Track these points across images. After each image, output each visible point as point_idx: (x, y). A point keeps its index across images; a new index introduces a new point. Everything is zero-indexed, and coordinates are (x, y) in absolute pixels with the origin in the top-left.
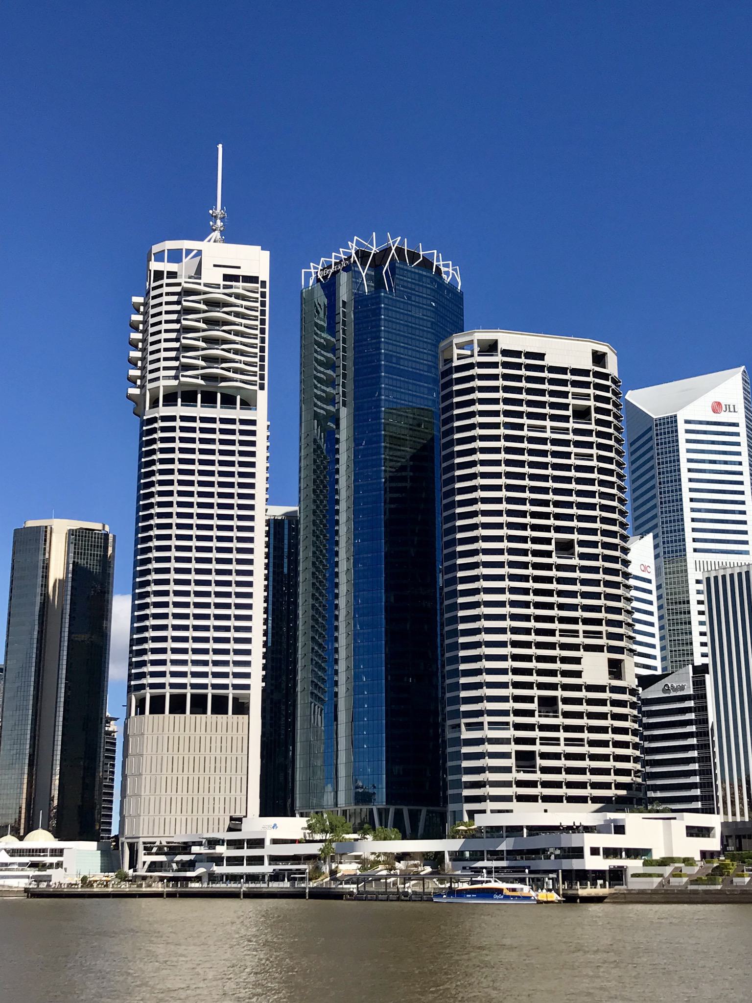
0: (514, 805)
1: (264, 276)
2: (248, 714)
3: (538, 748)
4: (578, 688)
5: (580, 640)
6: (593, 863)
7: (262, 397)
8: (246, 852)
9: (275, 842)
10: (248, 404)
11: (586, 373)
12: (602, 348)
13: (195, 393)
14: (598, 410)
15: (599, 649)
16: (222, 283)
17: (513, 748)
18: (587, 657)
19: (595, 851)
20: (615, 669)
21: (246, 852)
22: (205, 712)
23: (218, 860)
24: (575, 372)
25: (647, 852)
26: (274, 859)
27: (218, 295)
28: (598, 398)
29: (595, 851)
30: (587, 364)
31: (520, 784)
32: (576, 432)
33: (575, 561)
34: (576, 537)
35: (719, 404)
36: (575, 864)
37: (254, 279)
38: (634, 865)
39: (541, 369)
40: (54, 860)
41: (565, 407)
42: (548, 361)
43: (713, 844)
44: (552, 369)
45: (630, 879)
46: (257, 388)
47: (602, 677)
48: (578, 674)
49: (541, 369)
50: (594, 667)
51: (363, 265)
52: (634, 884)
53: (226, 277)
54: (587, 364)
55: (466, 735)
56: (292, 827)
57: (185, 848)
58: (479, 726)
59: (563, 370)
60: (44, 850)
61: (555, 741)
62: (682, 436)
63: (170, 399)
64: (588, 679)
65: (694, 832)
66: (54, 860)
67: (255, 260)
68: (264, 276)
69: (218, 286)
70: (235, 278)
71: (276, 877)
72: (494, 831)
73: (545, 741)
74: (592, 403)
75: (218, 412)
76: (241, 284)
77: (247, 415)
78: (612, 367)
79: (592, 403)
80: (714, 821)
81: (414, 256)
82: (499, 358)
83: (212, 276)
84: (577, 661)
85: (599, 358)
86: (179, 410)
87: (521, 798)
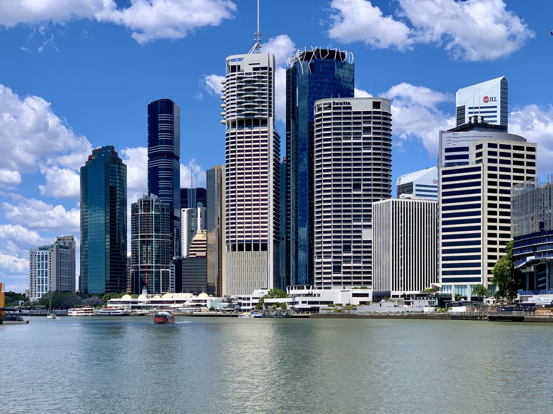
0: (332, 286)
2: (267, 250)
4: (360, 242)
8: (246, 302)
9: (253, 298)
11: (369, 113)
13: (243, 120)
16: (253, 72)
18: (364, 231)
19: (304, 302)
21: (246, 302)
22: (243, 250)
24: (365, 113)
25: (332, 302)
26: (253, 304)
29: (304, 302)
30: (370, 108)
31: (335, 278)
35: (486, 97)
39: (350, 113)
41: (360, 128)
44: (355, 113)
45: (320, 311)
46: (267, 117)
48: (360, 237)
53: (255, 69)
58: (320, 257)
59: (359, 113)
60: (202, 300)
64: (364, 239)
65: (355, 295)
66: (203, 304)
69: (250, 74)
70: (257, 69)
76: (260, 71)
79: (372, 125)
84: (360, 231)
87: (334, 283)
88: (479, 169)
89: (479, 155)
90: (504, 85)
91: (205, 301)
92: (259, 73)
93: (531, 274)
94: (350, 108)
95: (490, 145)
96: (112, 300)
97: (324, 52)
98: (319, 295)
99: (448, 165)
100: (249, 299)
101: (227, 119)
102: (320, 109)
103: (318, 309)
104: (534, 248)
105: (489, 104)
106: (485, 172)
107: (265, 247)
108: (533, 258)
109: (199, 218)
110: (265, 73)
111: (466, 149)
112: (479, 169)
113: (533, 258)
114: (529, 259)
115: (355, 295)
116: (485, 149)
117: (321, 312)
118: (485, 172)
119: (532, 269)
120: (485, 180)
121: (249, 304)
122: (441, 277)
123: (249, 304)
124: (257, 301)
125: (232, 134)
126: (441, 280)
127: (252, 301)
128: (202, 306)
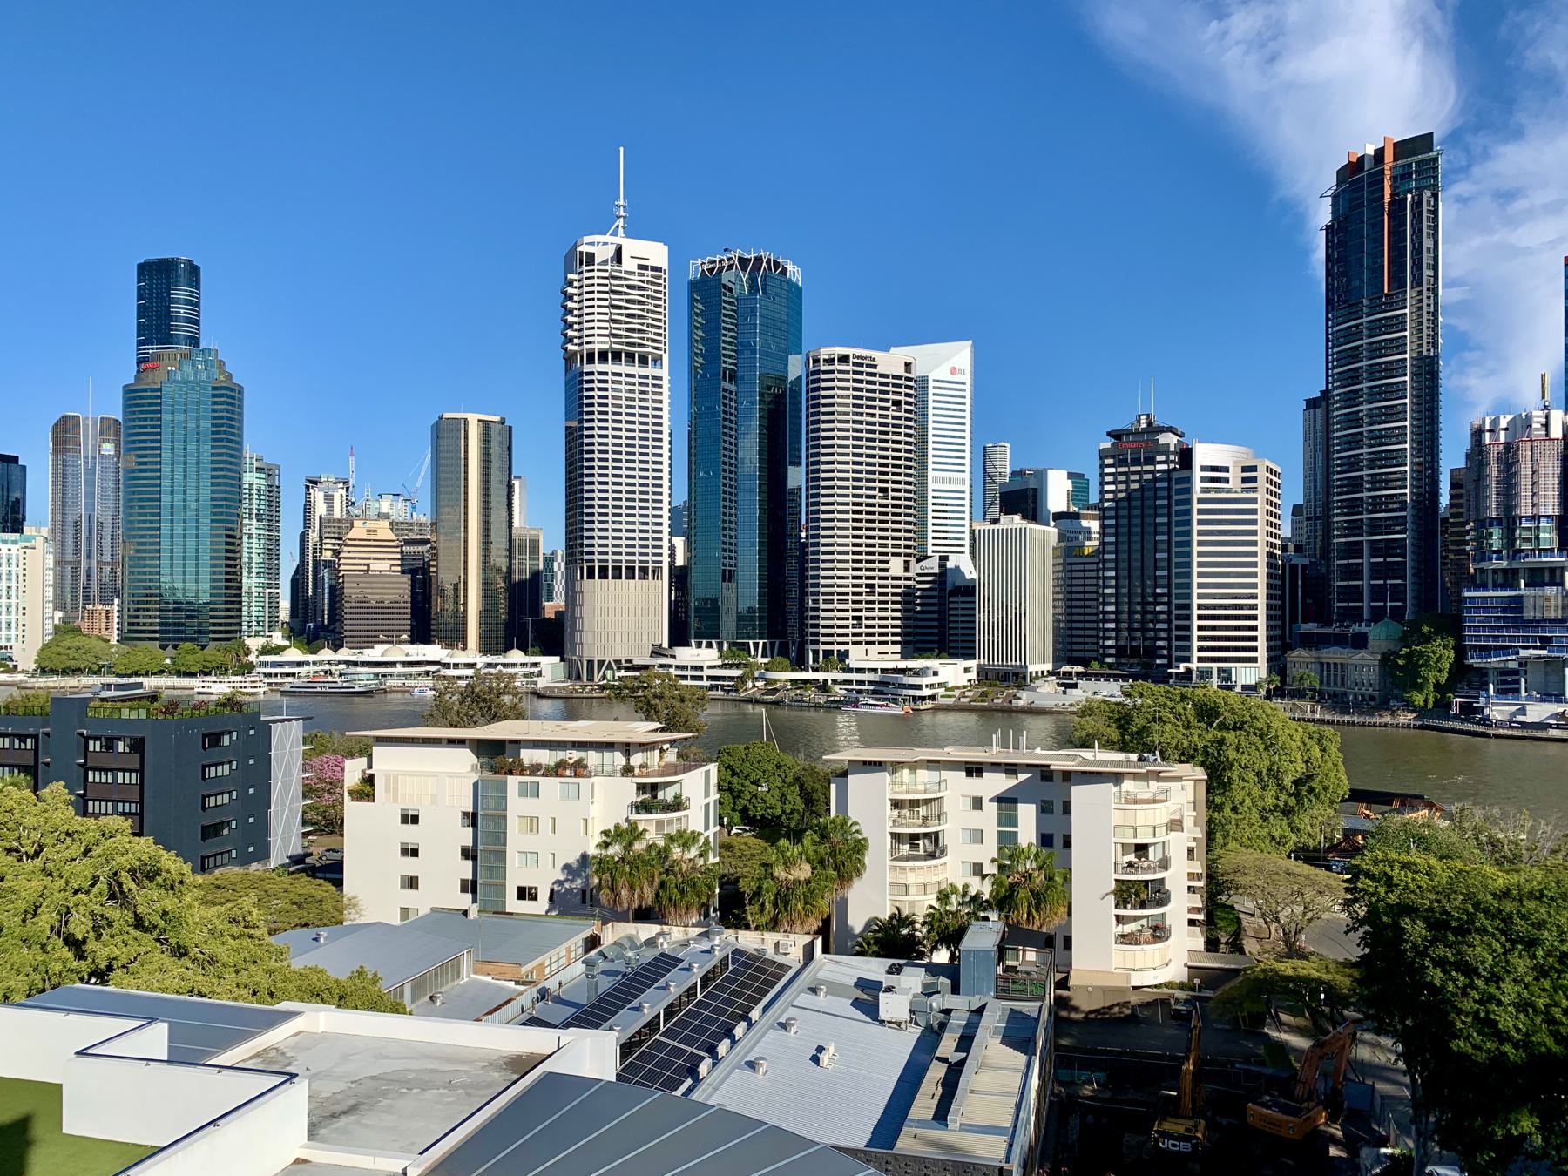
1: (665, 266)
3: (864, 614)
7: (666, 358)
9: (710, 667)
10: (657, 360)
11: (900, 378)
12: (909, 360)
14: (907, 403)
15: (899, 555)
17: (851, 614)
24: (894, 377)
26: (709, 678)
27: (635, 280)
28: (907, 395)
32: (894, 418)
33: (890, 501)
34: (890, 486)
36: (917, 693)
37: (658, 269)
39: (874, 375)
40: (536, 670)
41: (887, 401)
42: (879, 370)
44: (882, 376)
49: (874, 375)
50: (896, 566)
51: (744, 270)
52: (941, 701)
53: (640, 267)
54: (901, 372)
55: (822, 606)
59: (887, 376)
61: (873, 610)
62: (931, 391)
63: (603, 356)
64: (891, 573)
67: (657, 253)
68: (665, 266)
71: (712, 688)
73: (868, 610)
74: (903, 398)
75: (636, 369)
77: (656, 373)
80: (973, 664)
81: (777, 264)
82: (850, 368)
83: (629, 264)
94: (875, 367)
98: (936, 673)
100: (701, 668)
101: (586, 347)
105: (956, 378)
110: (659, 278)
111: (1226, 470)
122: (1196, 654)
125: (600, 373)
126: (1195, 659)
127: (706, 672)
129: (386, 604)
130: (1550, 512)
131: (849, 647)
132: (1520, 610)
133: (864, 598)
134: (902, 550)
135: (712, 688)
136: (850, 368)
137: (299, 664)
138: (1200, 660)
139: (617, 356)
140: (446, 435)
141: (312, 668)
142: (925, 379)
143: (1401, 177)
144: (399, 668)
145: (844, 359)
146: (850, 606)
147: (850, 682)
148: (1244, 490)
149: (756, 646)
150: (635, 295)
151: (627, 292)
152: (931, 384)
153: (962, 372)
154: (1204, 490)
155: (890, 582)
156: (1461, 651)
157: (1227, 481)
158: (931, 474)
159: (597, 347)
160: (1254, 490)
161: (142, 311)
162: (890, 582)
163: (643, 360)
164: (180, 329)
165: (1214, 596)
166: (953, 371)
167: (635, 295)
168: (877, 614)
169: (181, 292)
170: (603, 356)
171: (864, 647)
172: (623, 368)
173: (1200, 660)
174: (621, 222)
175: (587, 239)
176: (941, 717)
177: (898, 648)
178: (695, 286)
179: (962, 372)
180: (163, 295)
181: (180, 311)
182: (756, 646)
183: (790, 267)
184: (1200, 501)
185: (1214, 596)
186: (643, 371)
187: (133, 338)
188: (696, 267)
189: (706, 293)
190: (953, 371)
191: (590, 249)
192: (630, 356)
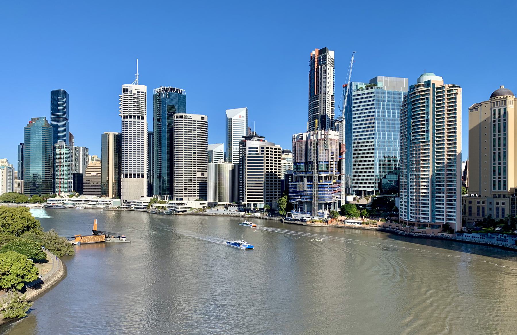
1: (145, 91)
5: (197, 170)
6: (180, 210)
7: (145, 117)
8: (139, 204)
10: (143, 118)
20: (203, 174)
21: (139, 204)
23: (135, 205)
27: (136, 96)
37: (143, 92)
38: (189, 209)
43: (206, 205)
47: (200, 176)
52: (188, 212)
53: (138, 92)
55: (176, 186)
56: (148, 199)
57: (130, 203)
65: (201, 204)
67: (143, 88)
68: (145, 91)
70: (139, 92)
71: (144, 208)
72: (172, 204)
74: (201, 127)
75: (137, 120)
78: (206, 120)
82: (183, 119)
83: (134, 92)
85: (203, 118)
86: (129, 120)
88: (263, 157)
89: (262, 151)
90: (247, 110)
91: (110, 201)
92: (140, 94)
93: (296, 205)
95: (268, 148)
96: (50, 199)
97: (174, 89)
99: (249, 154)
100: (141, 203)
102: (177, 117)
103: (186, 211)
104: (301, 196)
105: (241, 119)
106: (265, 159)
107: (143, 176)
108: (300, 200)
109: (81, 152)
111: (257, 148)
112: (263, 157)
113: (300, 200)
114: (298, 200)
115: (201, 204)
116: (266, 149)
117: (188, 212)
118: (265, 159)
119: (298, 203)
120: (265, 161)
121: (141, 205)
122: (247, 200)
123: (141, 205)
124: (147, 204)
127: (143, 204)
128: (108, 204)
129: (95, 184)
130: (303, 161)
131: (183, 197)
132: (296, 188)
133: (188, 183)
134: (201, 170)
135: (144, 208)
136: (183, 119)
137: (59, 200)
138: (248, 201)
139: (131, 117)
140: (105, 138)
141: (61, 202)
142: (231, 119)
143: (319, 61)
144: (83, 202)
145: (181, 117)
146: (183, 186)
147: (170, 207)
148: (262, 154)
149: (167, 197)
150: (136, 100)
151: (134, 99)
152: (233, 121)
153: (243, 117)
154: (249, 154)
155: (197, 179)
156: (288, 199)
157: (257, 151)
158: (233, 147)
159: (125, 114)
160: (263, 154)
161: (52, 104)
162: (197, 179)
163: (138, 117)
164: (61, 109)
165: (252, 184)
166: (240, 117)
167: (136, 100)
168: (192, 188)
169: (61, 99)
170: (127, 117)
171: (188, 197)
172: (132, 120)
173: (248, 201)
174: (137, 79)
175: (123, 85)
176: (188, 217)
177: (198, 198)
178: (155, 96)
179: (243, 117)
180: (58, 98)
181: (61, 104)
182: (167, 197)
183: (183, 90)
184: (248, 157)
185: (252, 184)
186: (139, 120)
187: (50, 112)
188: (155, 91)
189: (157, 98)
190: (240, 117)
191: (127, 88)
192: (135, 116)
